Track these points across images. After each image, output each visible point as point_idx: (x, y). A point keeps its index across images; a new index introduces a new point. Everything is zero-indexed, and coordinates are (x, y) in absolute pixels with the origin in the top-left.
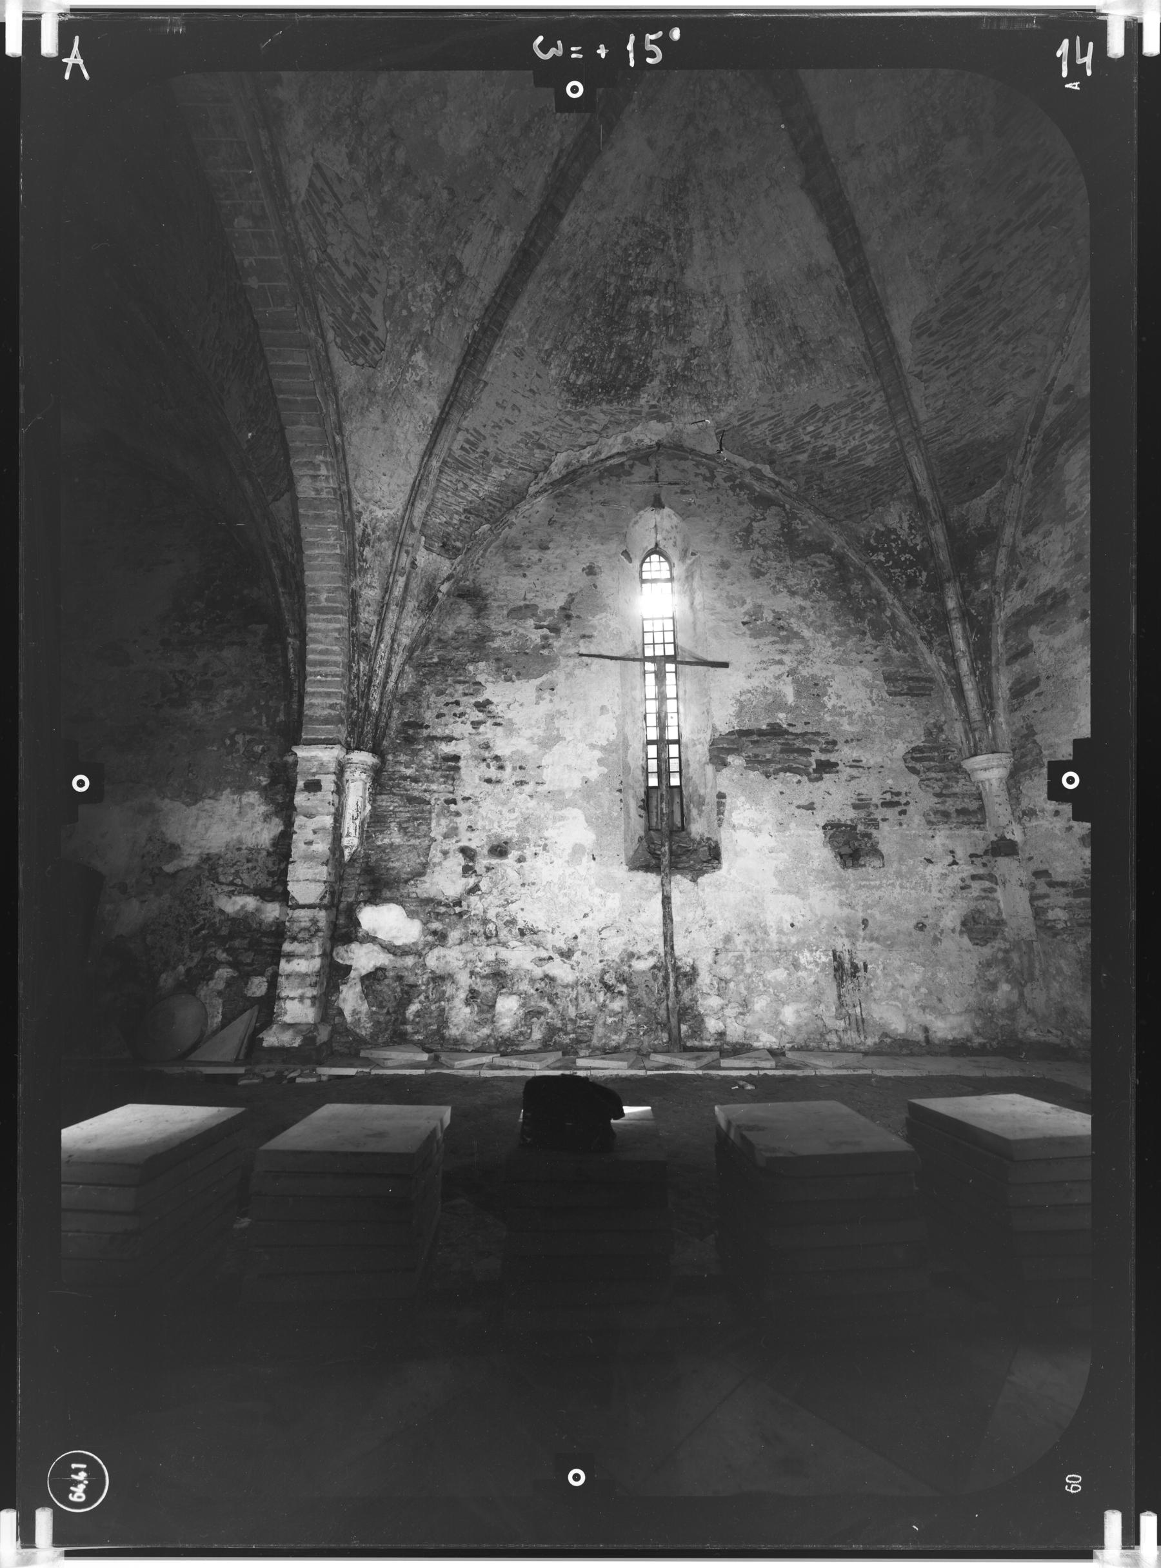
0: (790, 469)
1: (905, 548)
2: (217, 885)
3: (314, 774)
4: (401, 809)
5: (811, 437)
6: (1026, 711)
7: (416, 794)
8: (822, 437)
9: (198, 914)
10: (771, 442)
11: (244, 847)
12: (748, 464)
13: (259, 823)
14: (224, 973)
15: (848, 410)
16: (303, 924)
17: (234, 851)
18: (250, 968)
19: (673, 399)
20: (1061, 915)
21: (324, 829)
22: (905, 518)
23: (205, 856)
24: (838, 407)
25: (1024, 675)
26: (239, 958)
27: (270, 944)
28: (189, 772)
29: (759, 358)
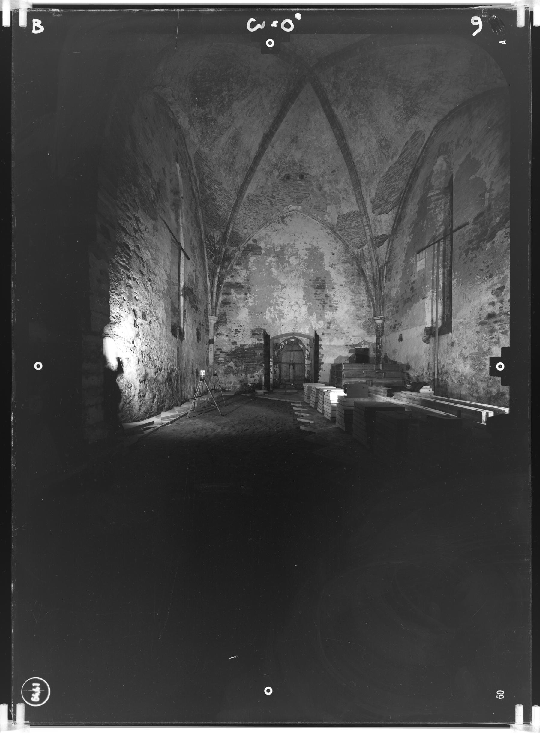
0: (203, 190)
1: (214, 246)
5: (214, 189)
6: (225, 308)
8: (217, 193)
10: (206, 176)
12: (196, 175)
15: (226, 195)
19: (198, 123)
20: (222, 359)
22: (218, 238)
24: (225, 190)
25: (227, 300)
29: (223, 150)
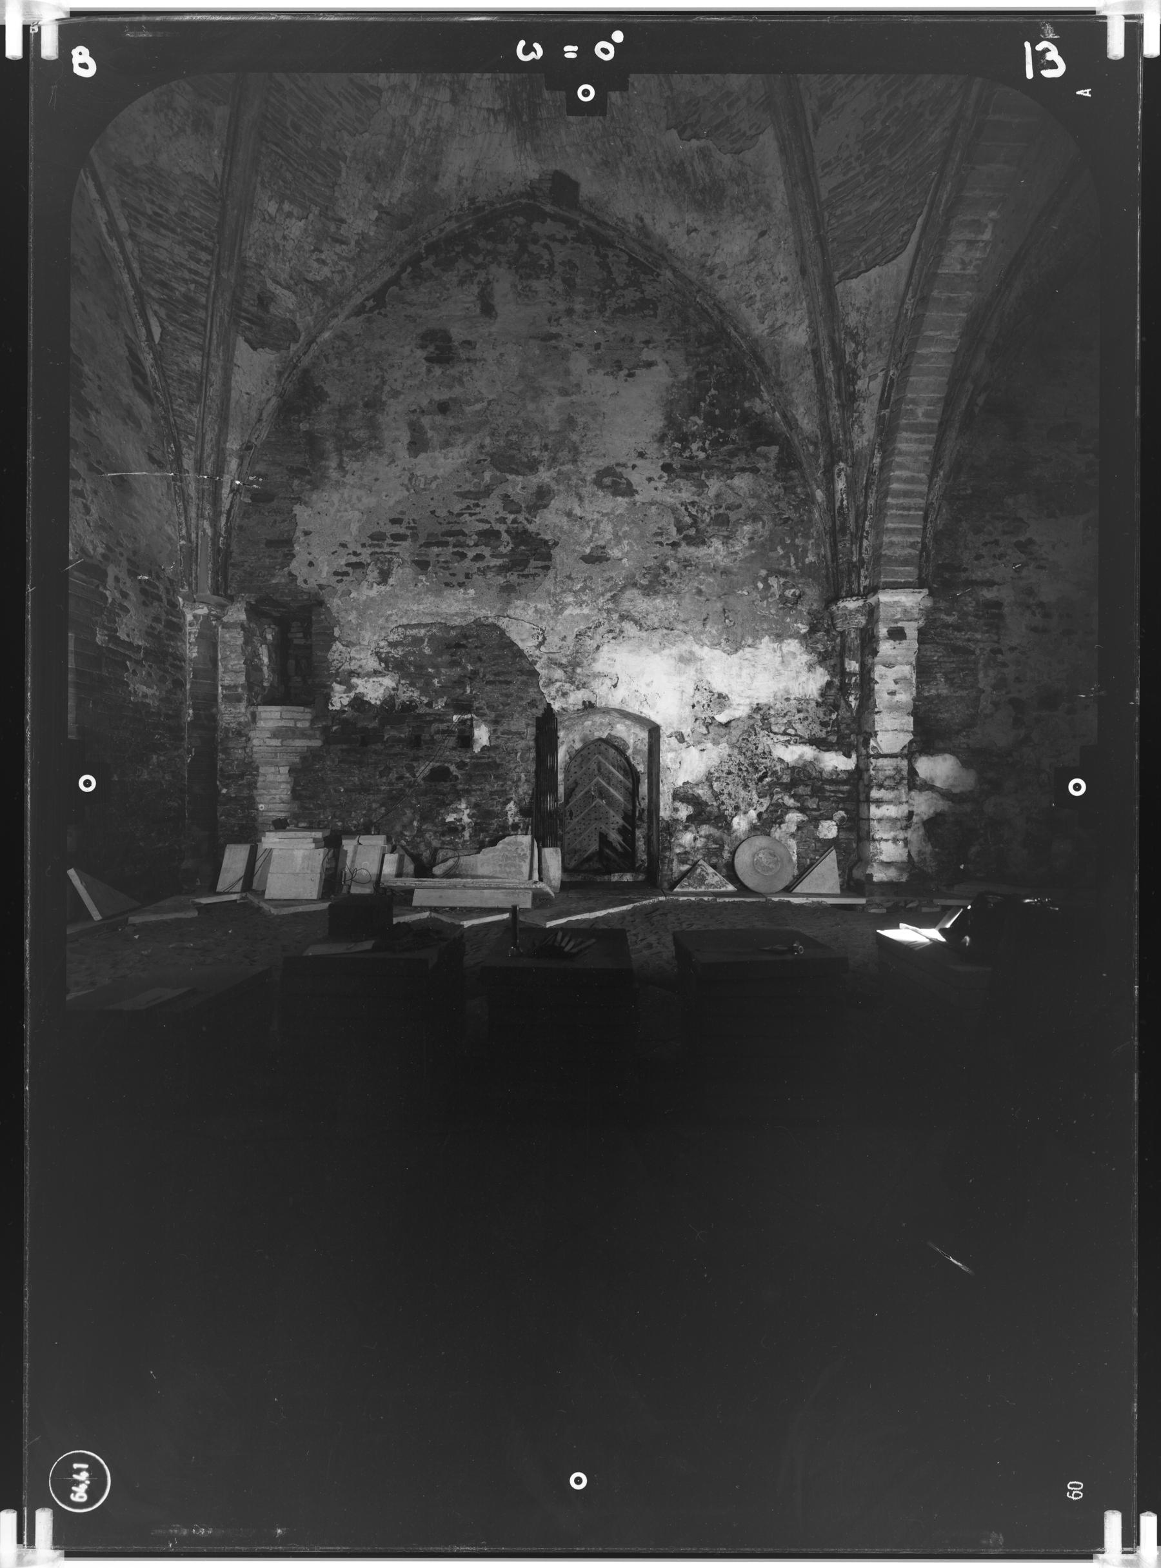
2: (772, 735)
3: (896, 621)
4: (945, 659)
7: (960, 643)
9: (759, 763)
11: (792, 697)
13: (804, 673)
14: (794, 817)
16: (888, 773)
17: (783, 701)
18: (817, 813)
21: (905, 679)
23: (755, 706)
26: (805, 804)
27: (832, 792)
28: (726, 618)
